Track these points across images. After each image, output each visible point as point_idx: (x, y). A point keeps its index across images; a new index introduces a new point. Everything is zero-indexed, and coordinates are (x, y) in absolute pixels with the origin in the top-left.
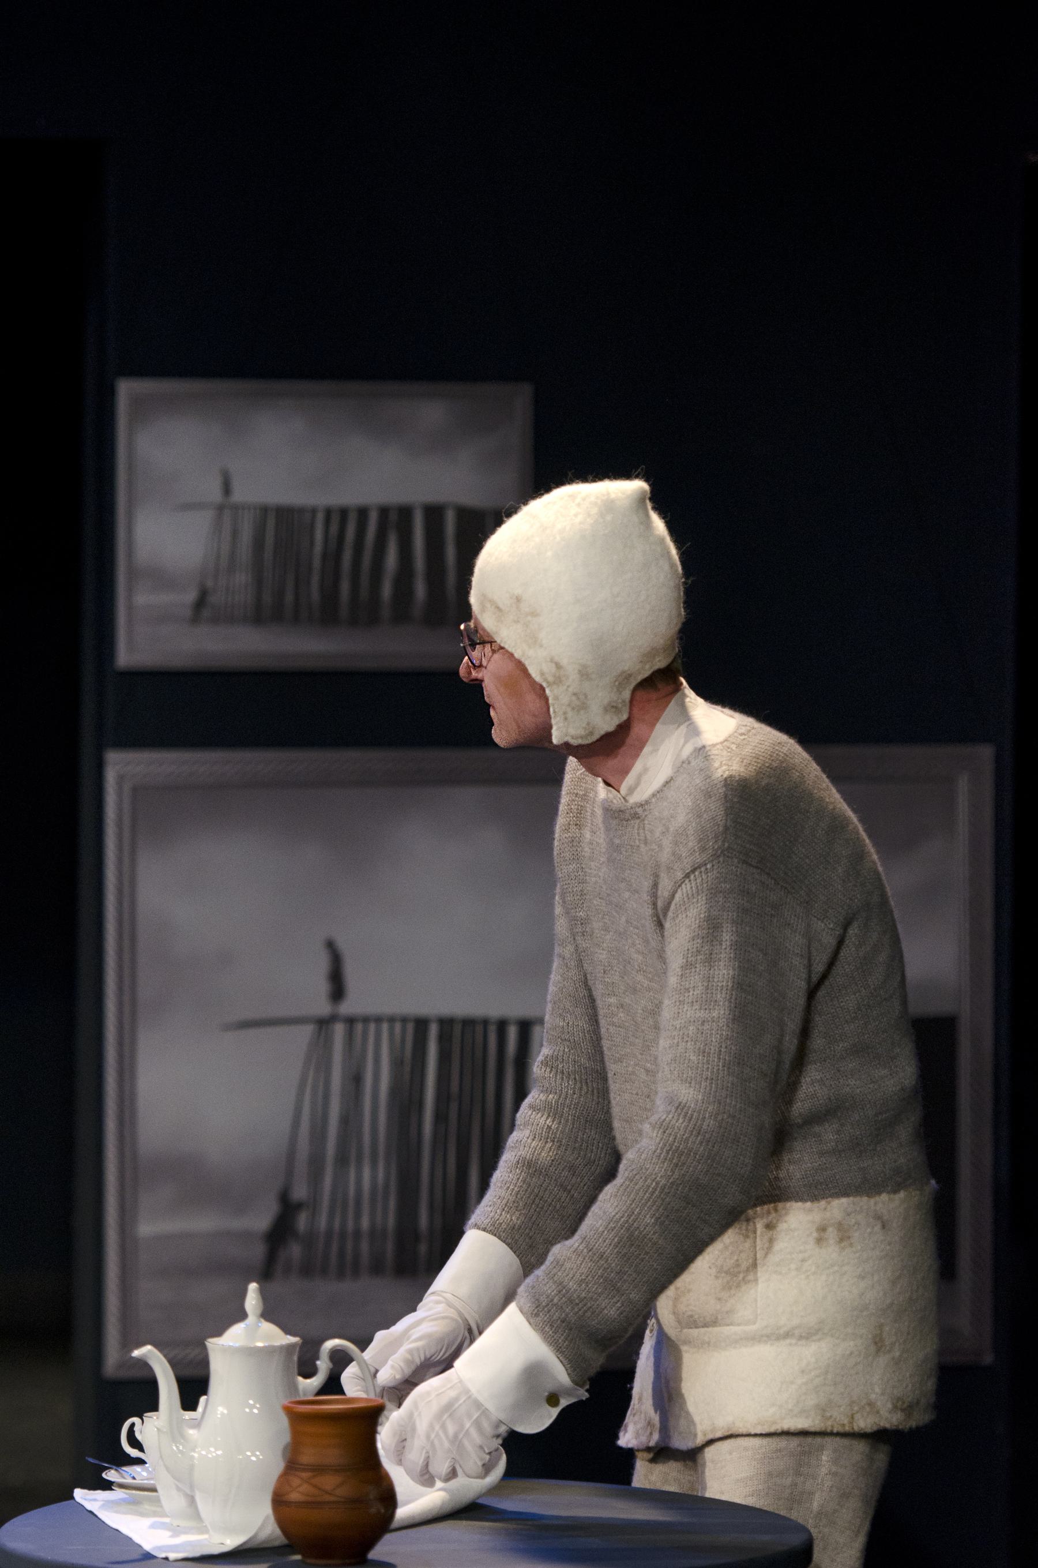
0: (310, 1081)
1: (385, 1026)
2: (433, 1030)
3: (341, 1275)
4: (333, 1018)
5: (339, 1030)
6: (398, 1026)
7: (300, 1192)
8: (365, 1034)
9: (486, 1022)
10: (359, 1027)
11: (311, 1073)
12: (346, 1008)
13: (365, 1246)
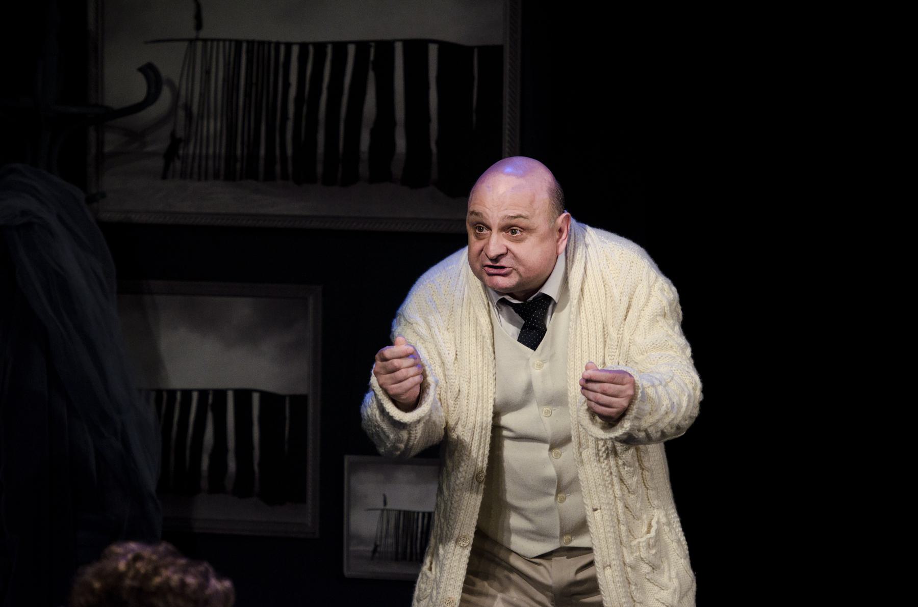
0: (185, 72)
1: (221, 44)
2: (244, 46)
3: (199, 180)
4: (197, 39)
5: (199, 44)
6: (227, 43)
7: (180, 133)
8: (212, 47)
9: (270, 43)
10: (209, 43)
11: (186, 68)
12: (203, 34)
13: (211, 163)
